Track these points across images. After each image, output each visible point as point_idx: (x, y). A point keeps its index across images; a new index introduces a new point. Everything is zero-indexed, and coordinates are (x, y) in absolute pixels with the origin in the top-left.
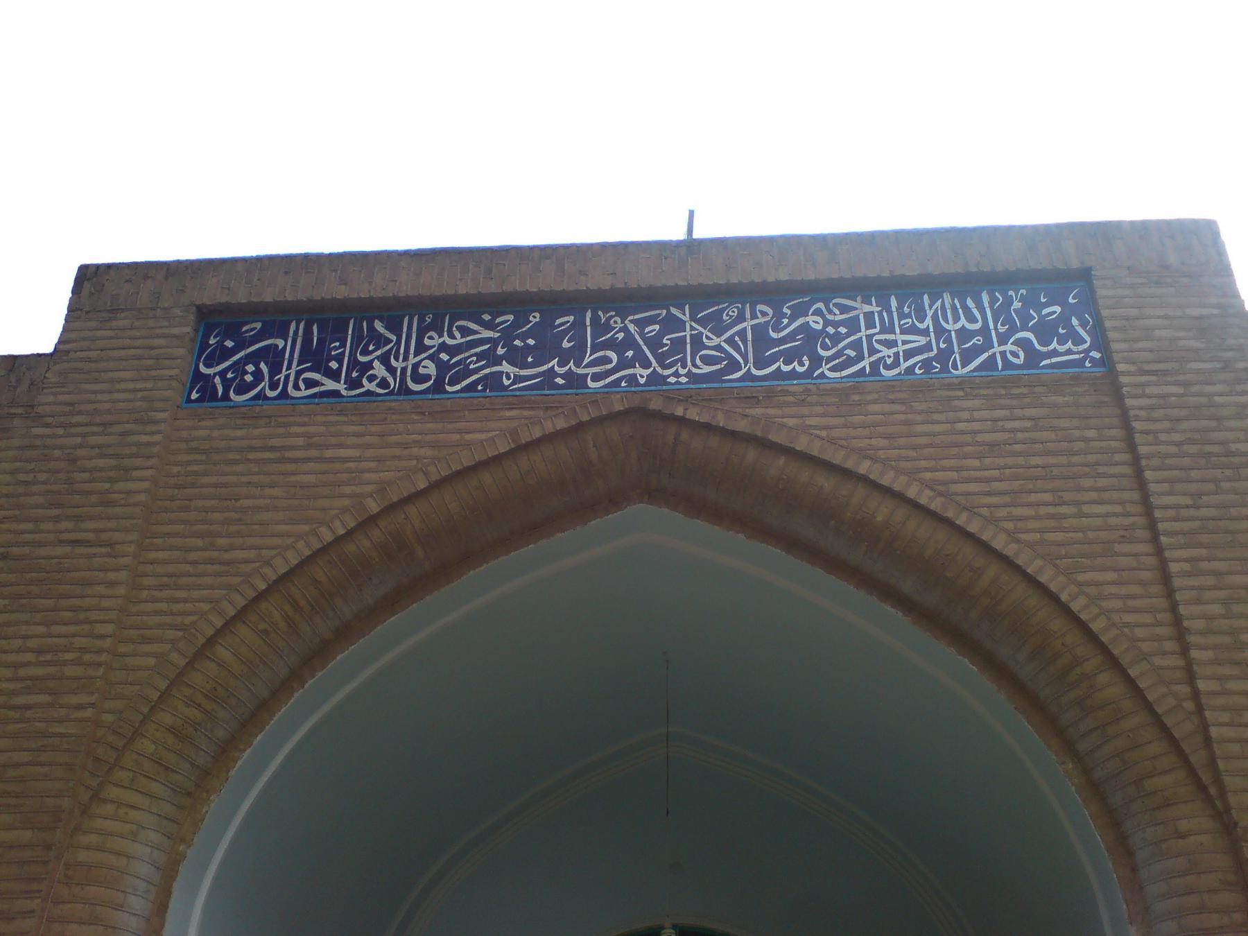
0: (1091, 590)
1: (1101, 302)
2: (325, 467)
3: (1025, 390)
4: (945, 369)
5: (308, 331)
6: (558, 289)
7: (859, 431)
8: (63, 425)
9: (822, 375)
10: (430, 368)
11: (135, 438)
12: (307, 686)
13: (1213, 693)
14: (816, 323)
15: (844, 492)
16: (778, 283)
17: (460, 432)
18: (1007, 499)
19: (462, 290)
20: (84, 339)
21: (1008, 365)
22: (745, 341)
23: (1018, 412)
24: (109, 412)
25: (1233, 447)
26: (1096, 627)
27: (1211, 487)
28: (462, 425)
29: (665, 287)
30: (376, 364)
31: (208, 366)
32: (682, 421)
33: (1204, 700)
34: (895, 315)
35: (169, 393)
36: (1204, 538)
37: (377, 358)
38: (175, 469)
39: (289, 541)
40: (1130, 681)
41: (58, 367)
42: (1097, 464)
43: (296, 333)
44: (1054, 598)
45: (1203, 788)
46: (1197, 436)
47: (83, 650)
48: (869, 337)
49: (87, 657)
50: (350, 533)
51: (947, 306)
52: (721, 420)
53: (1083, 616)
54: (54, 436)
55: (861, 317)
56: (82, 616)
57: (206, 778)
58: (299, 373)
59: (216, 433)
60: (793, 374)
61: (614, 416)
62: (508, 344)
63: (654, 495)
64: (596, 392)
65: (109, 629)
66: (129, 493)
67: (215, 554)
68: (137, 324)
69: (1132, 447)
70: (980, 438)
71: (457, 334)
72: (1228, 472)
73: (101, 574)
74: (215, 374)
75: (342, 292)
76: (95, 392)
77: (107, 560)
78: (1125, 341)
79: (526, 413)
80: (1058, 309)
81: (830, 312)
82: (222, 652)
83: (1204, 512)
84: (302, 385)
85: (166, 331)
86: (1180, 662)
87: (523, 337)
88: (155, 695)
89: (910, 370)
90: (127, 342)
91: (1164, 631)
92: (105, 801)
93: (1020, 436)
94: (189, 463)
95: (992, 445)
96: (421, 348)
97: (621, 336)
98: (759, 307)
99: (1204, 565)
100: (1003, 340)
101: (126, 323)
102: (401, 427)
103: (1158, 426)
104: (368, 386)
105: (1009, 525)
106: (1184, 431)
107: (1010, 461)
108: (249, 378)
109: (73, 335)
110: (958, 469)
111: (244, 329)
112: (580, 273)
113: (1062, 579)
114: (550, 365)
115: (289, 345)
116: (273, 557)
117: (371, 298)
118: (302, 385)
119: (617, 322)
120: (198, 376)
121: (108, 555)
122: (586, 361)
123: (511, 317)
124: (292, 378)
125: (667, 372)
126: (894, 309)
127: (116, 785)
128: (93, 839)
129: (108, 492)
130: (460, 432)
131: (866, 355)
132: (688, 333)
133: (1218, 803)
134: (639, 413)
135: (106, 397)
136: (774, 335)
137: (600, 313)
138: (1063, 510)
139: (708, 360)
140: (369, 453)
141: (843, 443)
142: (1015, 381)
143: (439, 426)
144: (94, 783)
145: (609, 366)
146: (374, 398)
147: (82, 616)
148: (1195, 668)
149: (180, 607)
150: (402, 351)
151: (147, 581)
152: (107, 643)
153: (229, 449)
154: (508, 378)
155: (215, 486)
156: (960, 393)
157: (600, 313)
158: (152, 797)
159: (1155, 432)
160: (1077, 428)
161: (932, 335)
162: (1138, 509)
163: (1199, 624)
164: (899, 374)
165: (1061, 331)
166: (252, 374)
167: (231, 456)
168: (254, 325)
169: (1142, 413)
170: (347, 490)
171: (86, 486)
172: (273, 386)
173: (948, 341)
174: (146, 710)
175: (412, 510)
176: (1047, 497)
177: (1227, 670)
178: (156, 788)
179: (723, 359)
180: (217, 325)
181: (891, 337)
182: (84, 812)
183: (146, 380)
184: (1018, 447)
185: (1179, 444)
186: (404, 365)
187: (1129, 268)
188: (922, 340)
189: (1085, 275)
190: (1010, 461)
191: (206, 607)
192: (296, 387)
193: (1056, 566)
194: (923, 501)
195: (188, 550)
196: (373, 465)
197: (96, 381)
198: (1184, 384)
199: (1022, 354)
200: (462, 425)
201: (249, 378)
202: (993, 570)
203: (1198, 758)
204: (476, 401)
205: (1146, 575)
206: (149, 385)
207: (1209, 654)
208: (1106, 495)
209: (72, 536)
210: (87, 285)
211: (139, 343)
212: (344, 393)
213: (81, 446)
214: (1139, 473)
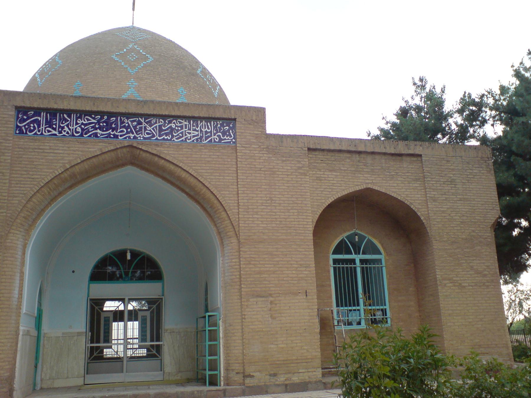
2: (55, 155)
4: (201, 141)
6: (112, 111)
9: (174, 140)
10: (79, 130)
11: (4, 144)
19: (87, 109)
23: (215, 154)
30: (65, 127)
31: (20, 123)
32: (141, 149)
36: (247, 186)
38: (16, 153)
44: (216, 196)
48: (185, 131)
50: (62, 172)
52: (150, 150)
58: (45, 128)
59: (25, 144)
60: (167, 140)
61: (125, 147)
62: (99, 124)
63: (133, 164)
64: (121, 140)
66: (5, 160)
67: (30, 176)
70: (206, 159)
75: (55, 106)
79: (104, 144)
80: (228, 128)
82: (34, 200)
87: (103, 122)
88: (20, 210)
89: (193, 141)
91: (236, 205)
95: (208, 161)
96: (77, 124)
97: (127, 125)
98: (161, 120)
99: (246, 192)
100: (214, 135)
102: (73, 146)
107: (211, 165)
108: (32, 128)
112: (118, 107)
115: (42, 118)
119: (126, 121)
120: (17, 127)
123: (99, 117)
125: (138, 136)
134: (131, 146)
136: (163, 128)
138: (221, 177)
139: (148, 134)
140: (66, 152)
149: (22, 189)
152: (6, 198)
153: (29, 148)
155: (28, 158)
158: (21, 231)
167: (30, 150)
170: (61, 161)
172: (39, 131)
173: (203, 134)
175: (76, 167)
176: (218, 174)
177: (245, 213)
178: (21, 230)
183: (4, 127)
184: (214, 162)
185: (246, 165)
188: (197, 133)
190: (211, 165)
192: (45, 132)
195: (22, 174)
196: (67, 155)
198: (250, 150)
201: (32, 128)
202: (205, 189)
205: (234, 193)
206: (5, 129)
214: (237, 170)
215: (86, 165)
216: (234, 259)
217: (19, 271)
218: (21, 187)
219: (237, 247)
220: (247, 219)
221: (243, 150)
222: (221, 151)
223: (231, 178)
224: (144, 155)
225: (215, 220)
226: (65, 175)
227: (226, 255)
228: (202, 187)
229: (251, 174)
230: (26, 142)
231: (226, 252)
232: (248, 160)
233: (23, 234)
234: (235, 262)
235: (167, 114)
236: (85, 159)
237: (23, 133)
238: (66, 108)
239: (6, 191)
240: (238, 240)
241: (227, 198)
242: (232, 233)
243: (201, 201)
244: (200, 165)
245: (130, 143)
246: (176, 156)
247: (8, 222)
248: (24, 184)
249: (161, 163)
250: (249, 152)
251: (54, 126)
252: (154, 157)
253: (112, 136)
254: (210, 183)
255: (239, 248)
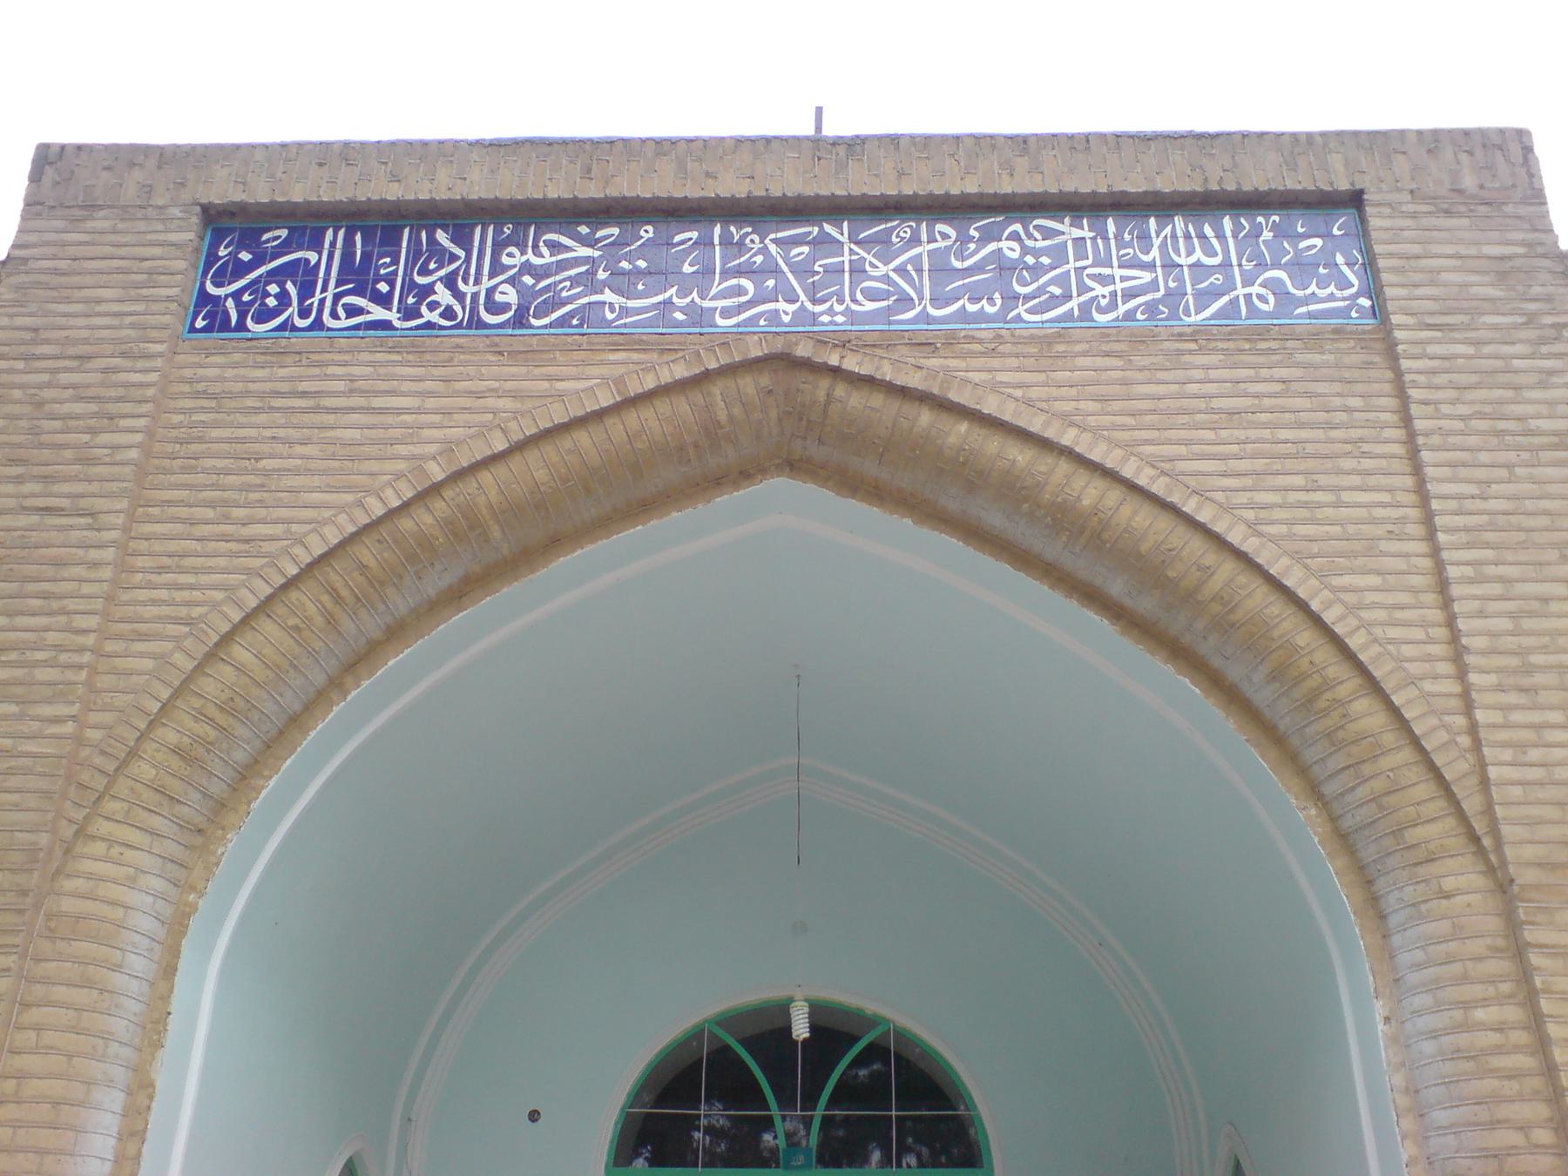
0: (1350, 598)
1: (1374, 235)
3: (1274, 345)
4: (1174, 315)
5: (349, 242)
6: (678, 194)
7: (1064, 391)
8: (25, 358)
9: (1018, 318)
11: (123, 377)
12: (349, 698)
13: (1494, 726)
14: (1011, 250)
15: (1043, 469)
16: (964, 196)
17: (550, 379)
18: (1248, 481)
19: (553, 194)
20: (47, 244)
21: (1253, 311)
22: (919, 271)
23: (1264, 373)
24: (86, 341)
25: (1533, 424)
26: (1354, 643)
27: (1504, 473)
28: (551, 370)
29: (817, 196)
30: (439, 287)
31: (218, 285)
32: (836, 371)
33: (1482, 735)
34: (1113, 242)
35: (167, 319)
36: (1490, 536)
37: (441, 279)
38: (177, 419)
39: (327, 514)
40: (1395, 711)
41: (14, 280)
42: (1361, 440)
43: (333, 244)
44: (1302, 606)
45: (1475, 839)
46: (1488, 409)
47: (59, 648)
49: (63, 657)
50: (406, 506)
51: (1179, 233)
52: (887, 373)
53: (1338, 629)
54: (11, 371)
55: (1070, 244)
56: (55, 605)
57: (222, 810)
58: (337, 297)
59: (229, 373)
60: (981, 316)
63: (796, 466)
65: (92, 622)
66: (116, 447)
68: (121, 226)
69: (1407, 421)
70: (1216, 403)
71: (545, 250)
72: (1525, 455)
73: (81, 552)
74: (227, 296)
75: (393, 193)
76: (65, 315)
77: (85, 533)
78: (1403, 286)
79: (635, 356)
80: (1318, 242)
81: (1030, 236)
82: (240, 653)
83: (1493, 504)
84: (341, 312)
85: (162, 237)
86: (1457, 689)
88: (155, 707)
89: (1130, 315)
90: (108, 250)
91: (1438, 650)
92: (93, 838)
93: (1267, 402)
94: (192, 411)
97: (759, 259)
98: (940, 227)
99: (1491, 570)
100: (1248, 282)
101: (106, 224)
102: (471, 370)
103: (1440, 395)
104: (428, 315)
105: (1250, 515)
106: (1472, 402)
107: (1253, 434)
108: (271, 302)
109: (33, 238)
110: (1188, 443)
111: (265, 237)
112: (708, 175)
113: (1314, 582)
114: (667, 295)
115: (325, 258)
116: (306, 534)
117: (432, 200)
118: (341, 312)
120: (204, 298)
121: (90, 528)
122: (714, 291)
123: (616, 231)
124: (328, 303)
126: (1111, 235)
127: (108, 819)
128: (78, 884)
129: (87, 445)
130: (550, 379)
131: (1075, 294)
132: (846, 258)
133: (1493, 858)
134: (783, 362)
135: (81, 322)
136: (957, 264)
137: (733, 229)
139: (872, 296)
140: (431, 403)
141: (1044, 405)
142: (1261, 333)
143: (523, 370)
144: (79, 815)
145: (744, 299)
146: (435, 332)
147: (55, 605)
148: (1474, 695)
149: (186, 595)
150: (473, 271)
151: (140, 562)
152: (90, 640)
153: (247, 394)
154: (612, 311)
155: (229, 441)
156: (1193, 346)
157: (733, 229)
158: (153, 833)
159: (1436, 403)
160: (1339, 395)
161: (1159, 270)
162: (1412, 498)
163: (1479, 642)
164: (1117, 319)
165: (1322, 270)
166: (276, 296)
167: (249, 403)
168: (277, 233)
169: (1422, 379)
170: (403, 450)
171: (59, 438)
172: (304, 313)
173: (1180, 280)
174: (143, 726)
175: (485, 477)
176: (1298, 481)
178: (157, 822)
179: (887, 295)
180: (230, 230)
181: (1106, 271)
182: (67, 852)
184: (1264, 417)
186: (475, 289)
187: (1412, 192)
188: (1147, 277)
189: (1355, 200)
190: (1253, 434)
191: (219, 595)
193: (1306, 567)
194: (1142, 481)
196: (437, 418)
197: (68, 300)
198: (1476, 343)
199: (1271, 299)
200: (551, 370)
201: (271, 302)
202: (1227, 569)
203: (1472, 805)
204: (570, 339)
205: (1417, 580)
207: (1492, 679)
208: (1372, 481)
209: (40, 502)
210: (49, 171)
211: (123, 251)
212: (397, 324)
213: (49, 385)
214: (1414, 453)
215: (537, 467)
216: (1485, 1002)
217: (120, 1074)
218: (180, 587)
219: (1494, 923)
220: (1529, 735)
221: (1429, 342)
222: (1299, 357)
223: (1385, 497)
224: (856, 401)
225: (1311, 755)
226: (424, 519)
227: (1413, 978)
228: (1211, 557)
229: (1509, 466)
230: (235, 366)
231: (1404, 959)
232: (1470, 395)
233: (173, 849)
234: (1500, 1028)
235: (971, 187)
236: (531, 431)
237: (225, 326)
238: (441, 195)
239: (98, 604)
240: (1491, 870)
241: (1379, 609)
242: (1439, 830)
243: (1207, 648)
244: (1183, 434)
245: (778, 346)
246: (1034, 393)
247: (85, 776)
248: (196, 571)
249: (952, 440)
250: (1471, 350)
251: (383, 287)
252: (910, 409)
253: (679, 316)
254: (1253, 527)
255: (1513, 926)
